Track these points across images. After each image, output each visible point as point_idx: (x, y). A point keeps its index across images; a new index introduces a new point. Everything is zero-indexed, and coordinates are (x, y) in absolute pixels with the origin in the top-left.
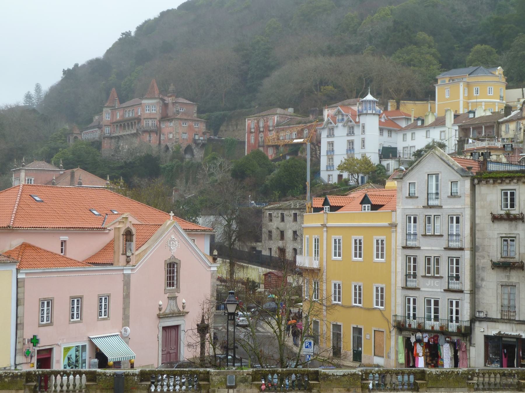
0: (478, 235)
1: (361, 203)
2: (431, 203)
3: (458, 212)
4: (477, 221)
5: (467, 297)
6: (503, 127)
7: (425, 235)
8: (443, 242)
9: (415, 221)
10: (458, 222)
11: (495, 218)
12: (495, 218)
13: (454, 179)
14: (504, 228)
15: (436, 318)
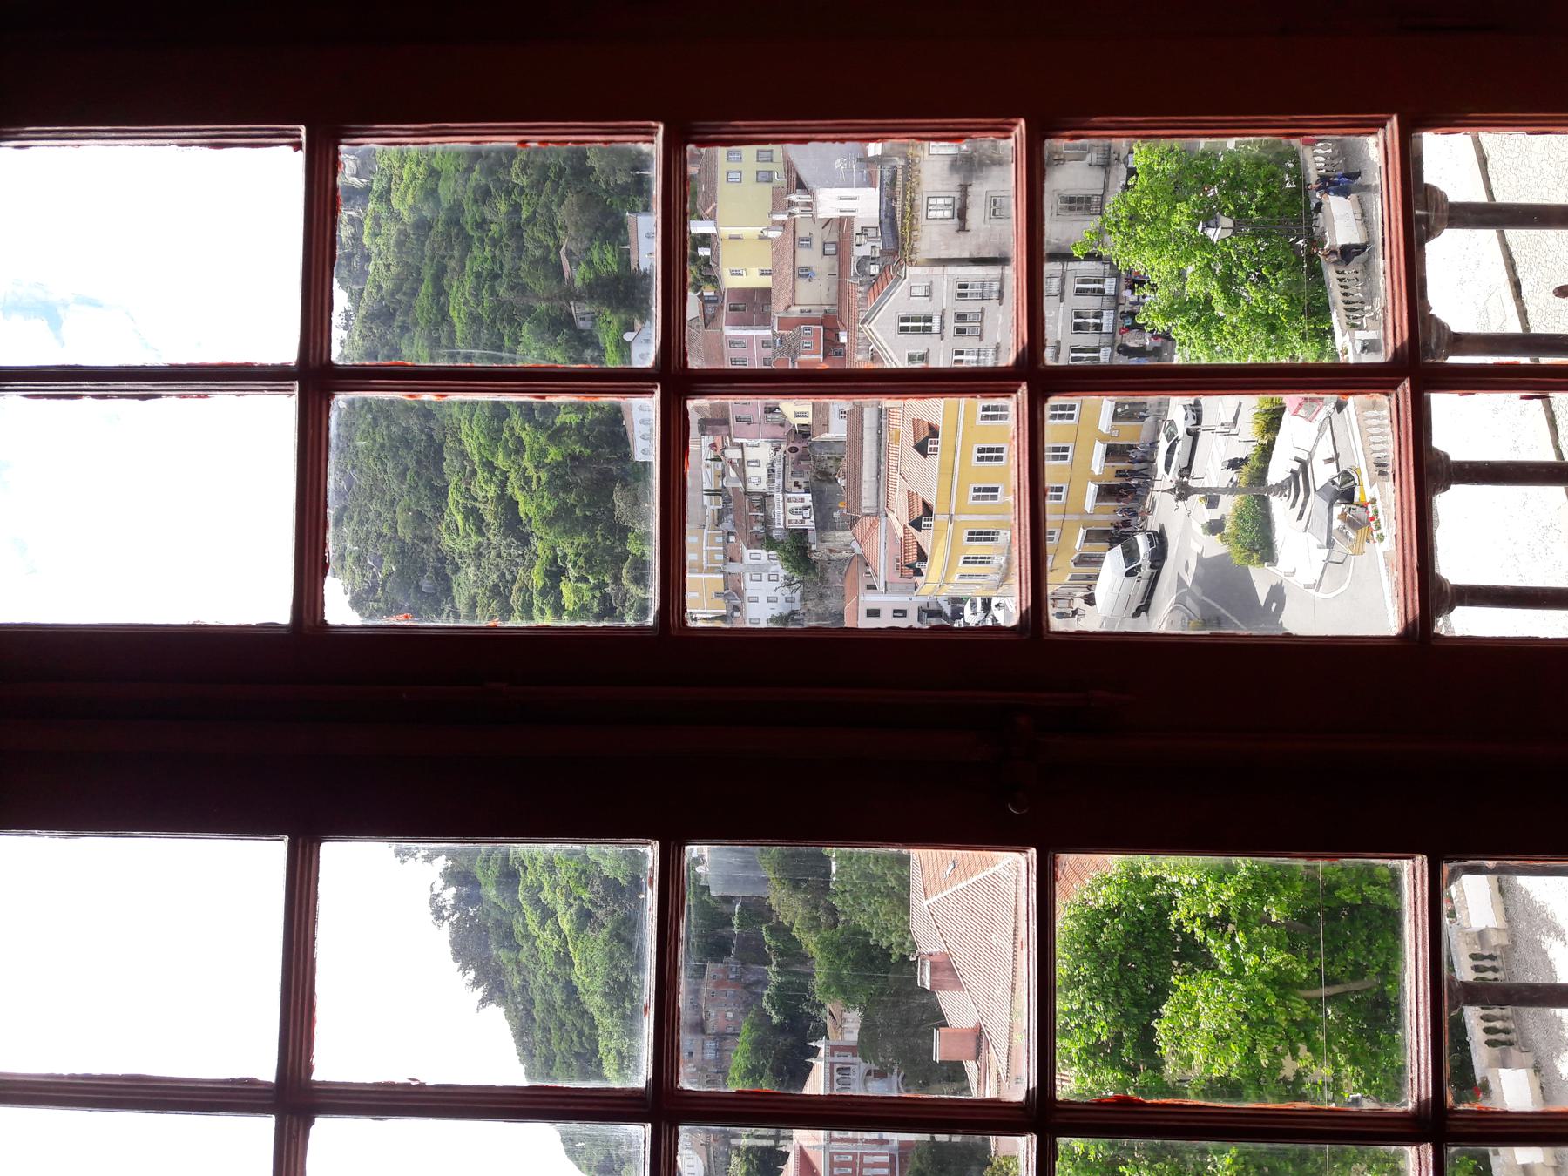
0: (985, 254)
1: (925, 454)
2: (936, 328)
3: (953, 288)
4: (966, 255)
5: (1071, 266)
6: (752, 487)
7: (981, 337)
8: (991, 305)
9: (961, 353)
10: (965, 287)
11: (963, 228)
12: (963, 228)
13: (907, 292)
14: (975, 216)
15: (1098, 315)
